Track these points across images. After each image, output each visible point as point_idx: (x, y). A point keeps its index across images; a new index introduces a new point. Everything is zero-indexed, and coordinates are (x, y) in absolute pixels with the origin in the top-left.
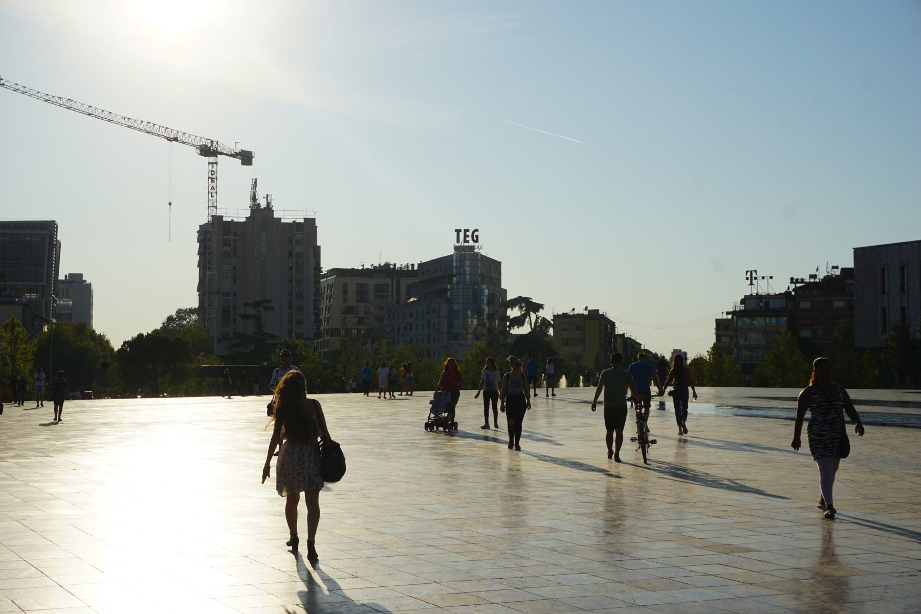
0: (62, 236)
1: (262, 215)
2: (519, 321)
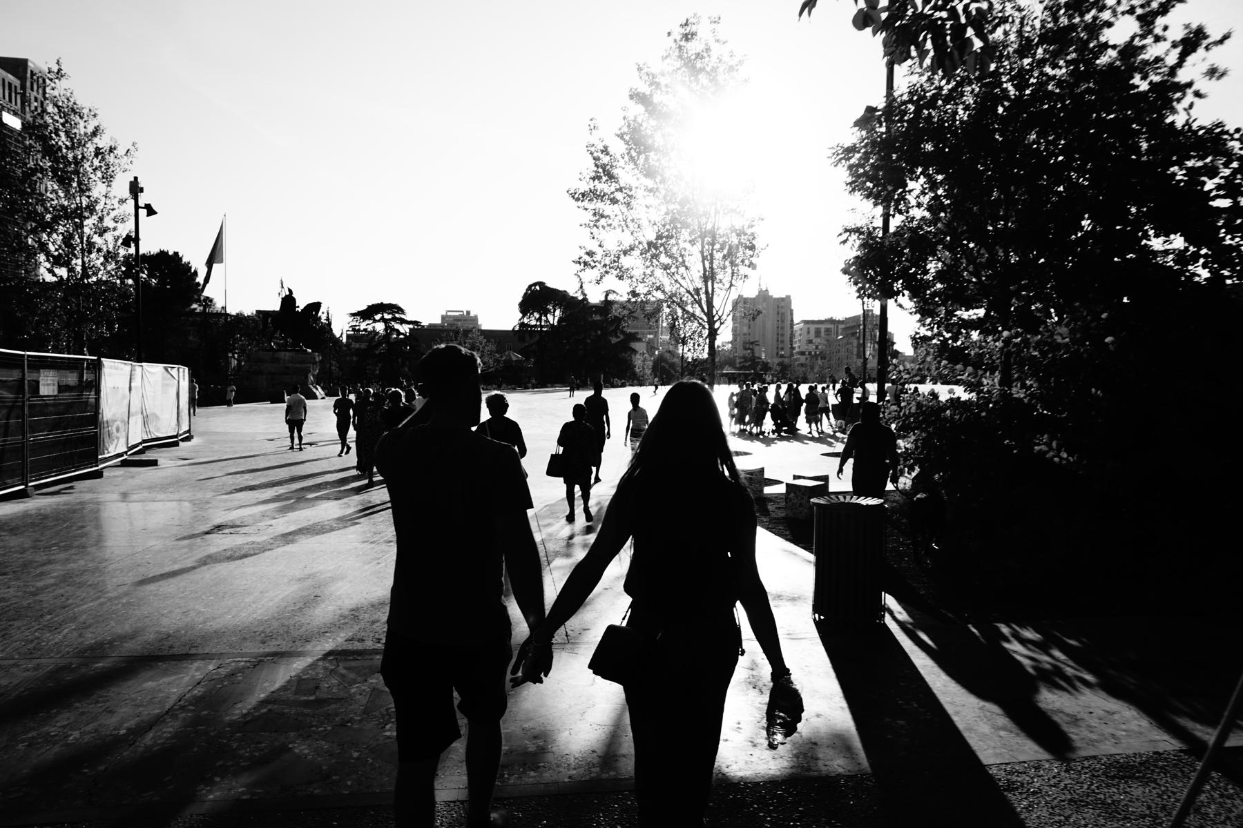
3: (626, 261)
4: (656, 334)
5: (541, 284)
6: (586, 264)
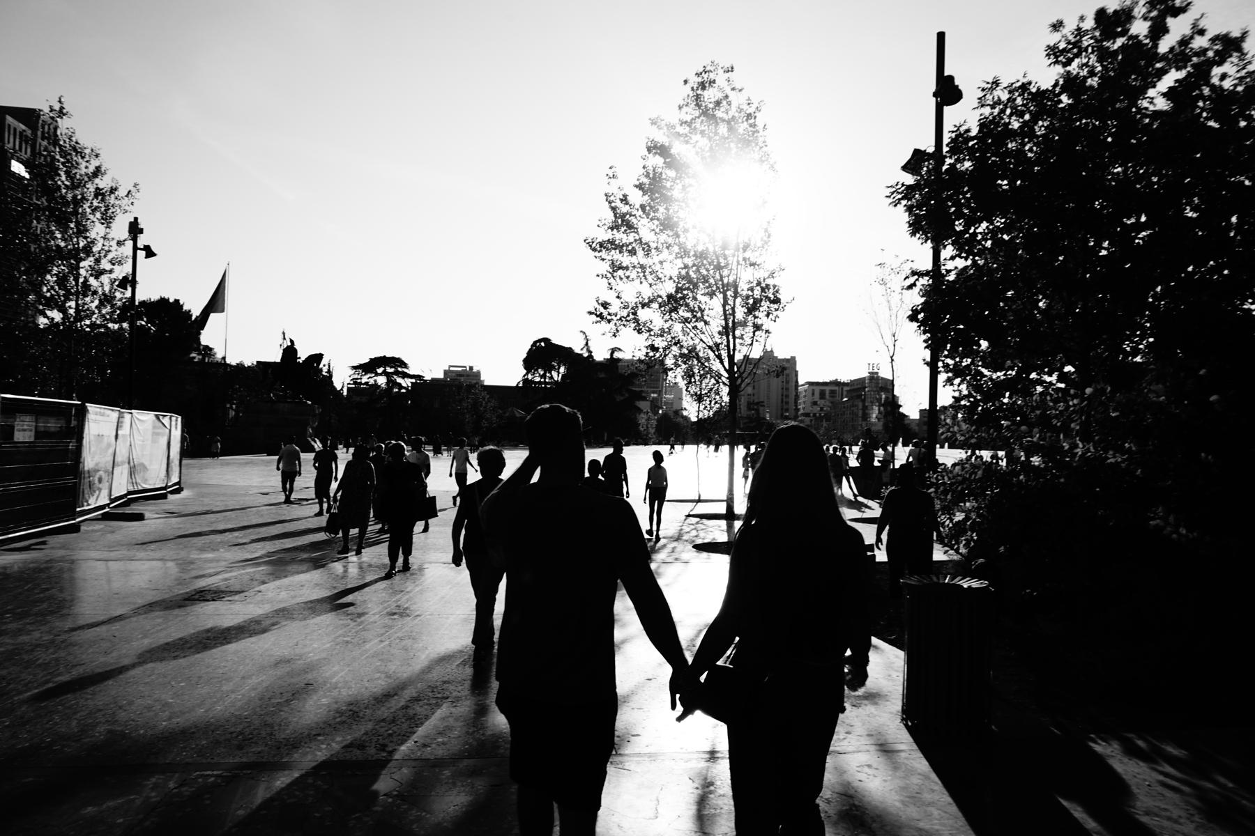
3: (644, 315)
4: (660, 393)
5: (546, 340)
6: (601, 316)
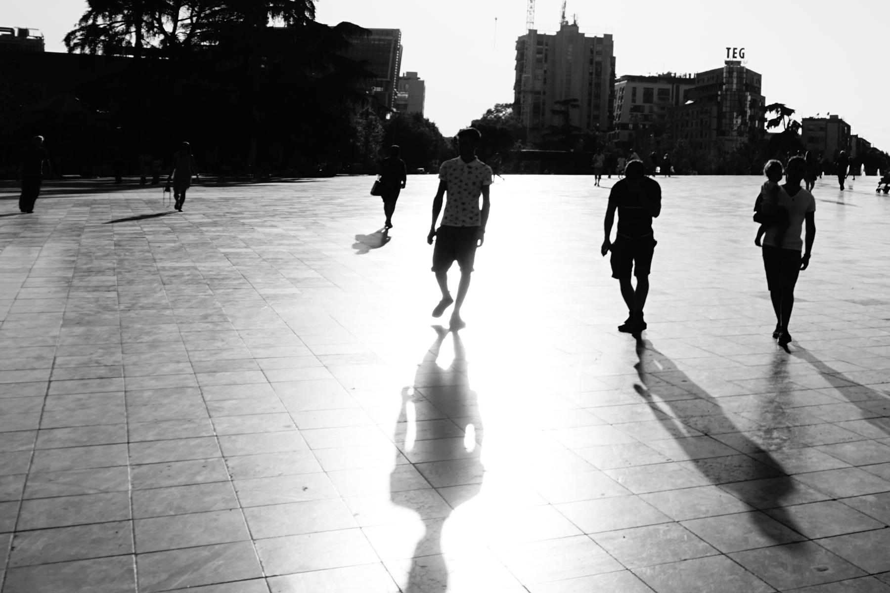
0: (404, 41)
1: (569, 31)
2: (775, 123)
4: (388, 86)
